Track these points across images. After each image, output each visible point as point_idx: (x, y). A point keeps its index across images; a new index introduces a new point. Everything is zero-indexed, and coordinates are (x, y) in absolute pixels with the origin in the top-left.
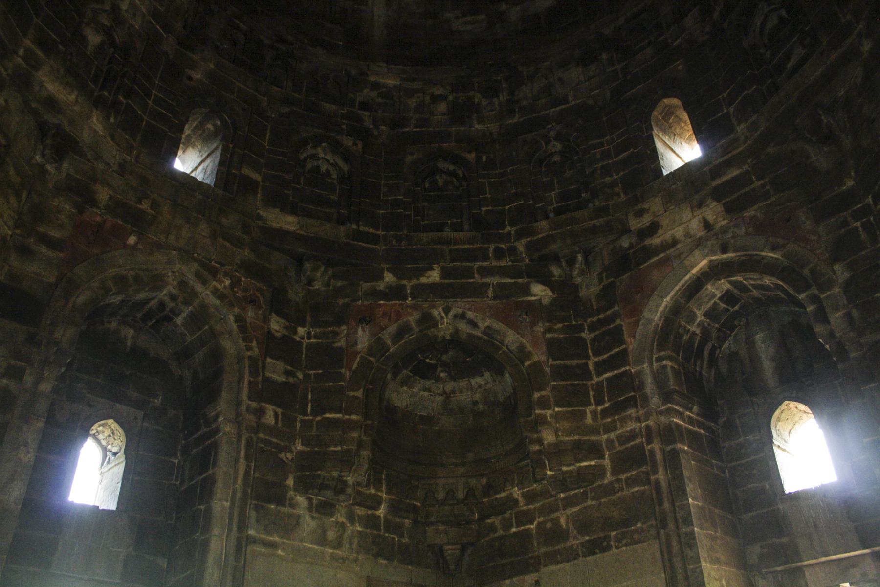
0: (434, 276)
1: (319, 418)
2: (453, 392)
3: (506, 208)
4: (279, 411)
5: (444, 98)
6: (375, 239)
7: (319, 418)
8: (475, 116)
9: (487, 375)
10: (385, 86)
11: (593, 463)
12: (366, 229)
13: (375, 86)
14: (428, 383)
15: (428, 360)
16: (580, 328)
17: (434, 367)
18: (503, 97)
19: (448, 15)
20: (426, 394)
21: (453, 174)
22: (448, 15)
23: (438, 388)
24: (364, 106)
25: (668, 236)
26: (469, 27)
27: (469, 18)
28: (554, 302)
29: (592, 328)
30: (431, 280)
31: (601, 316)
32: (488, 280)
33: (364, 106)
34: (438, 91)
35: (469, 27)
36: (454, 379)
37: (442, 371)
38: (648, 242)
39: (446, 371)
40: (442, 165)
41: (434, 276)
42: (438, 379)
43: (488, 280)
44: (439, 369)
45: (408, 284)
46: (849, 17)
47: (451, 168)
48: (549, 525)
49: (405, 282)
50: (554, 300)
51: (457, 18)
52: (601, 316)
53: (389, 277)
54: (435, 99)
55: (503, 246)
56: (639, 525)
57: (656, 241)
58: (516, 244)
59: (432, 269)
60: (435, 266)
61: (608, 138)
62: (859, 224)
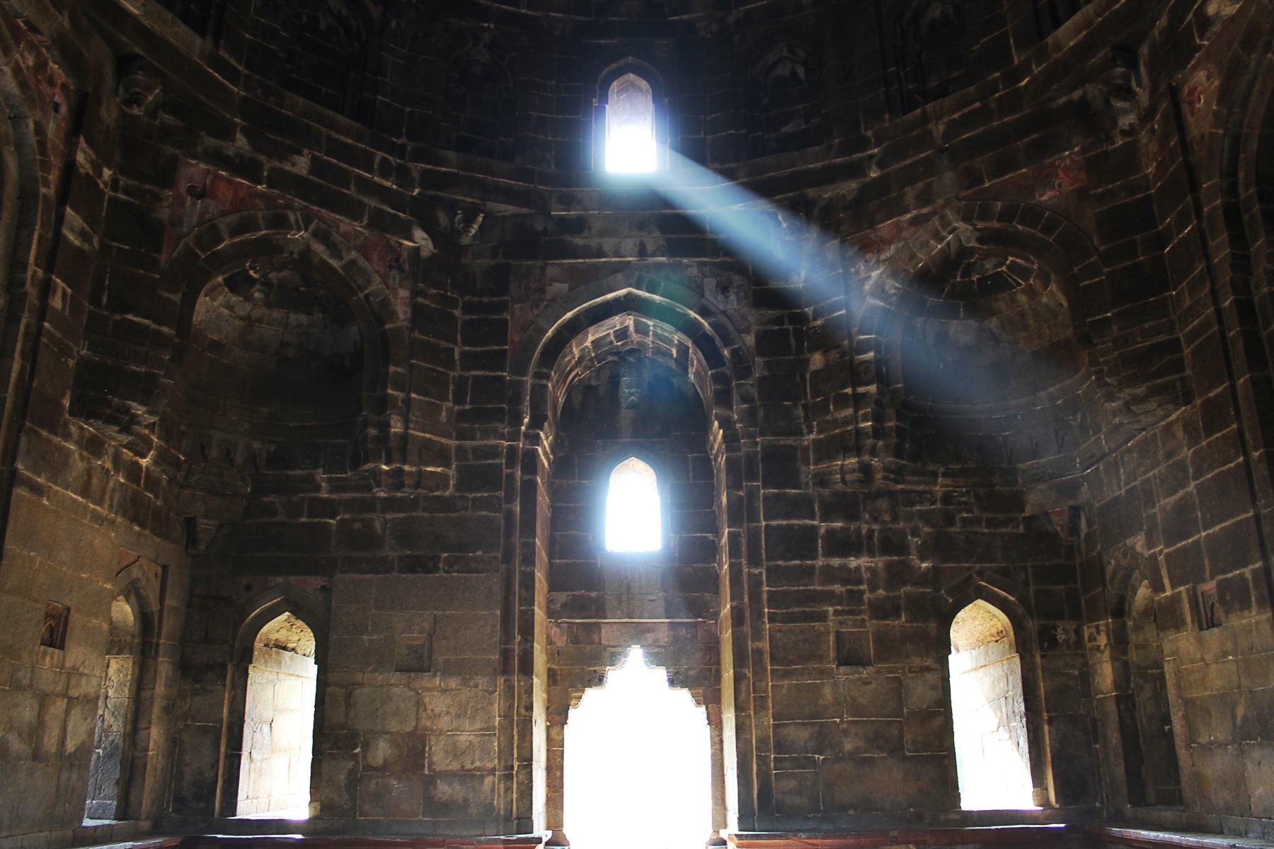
0: (301, 165)
1: (117, 317)
2: (260, 321)
3: (408, 109)
4: (69, 290)
6: (233, 75)
7: (117, 317)
9: (318, 316)
11: (439, 470)
12: (226, 56)
14: (234, 299)
15: (251, 272)
16: (453, 303)
17: (252, 281)
20: (226, 312)
23: (244, 308)
25: (594, 242)
28: (433, 258)
29: (468, 309)
30: (296, 170)
31: (485, 299)
32: (365, 200)
36: (268, 304)
37: (259, 290)
38: (567, 238)
39: (263, 292)
41: (301, 165)
42: (248, 298)
43: (365, 200)
44: (257, 286)
45: (268, 164)
46: (869, 133)
48: (357, 526)
49: (263, 158)
50: (434, 255)
52: (485, 299)
53: (241, 141)
55: (391, 158)
56: (479, 553)
57: (579, 241)
58: (410, 164)
59: (300, 154)
60: (306, 151)
61: (553, 83)
62: (791, 328)
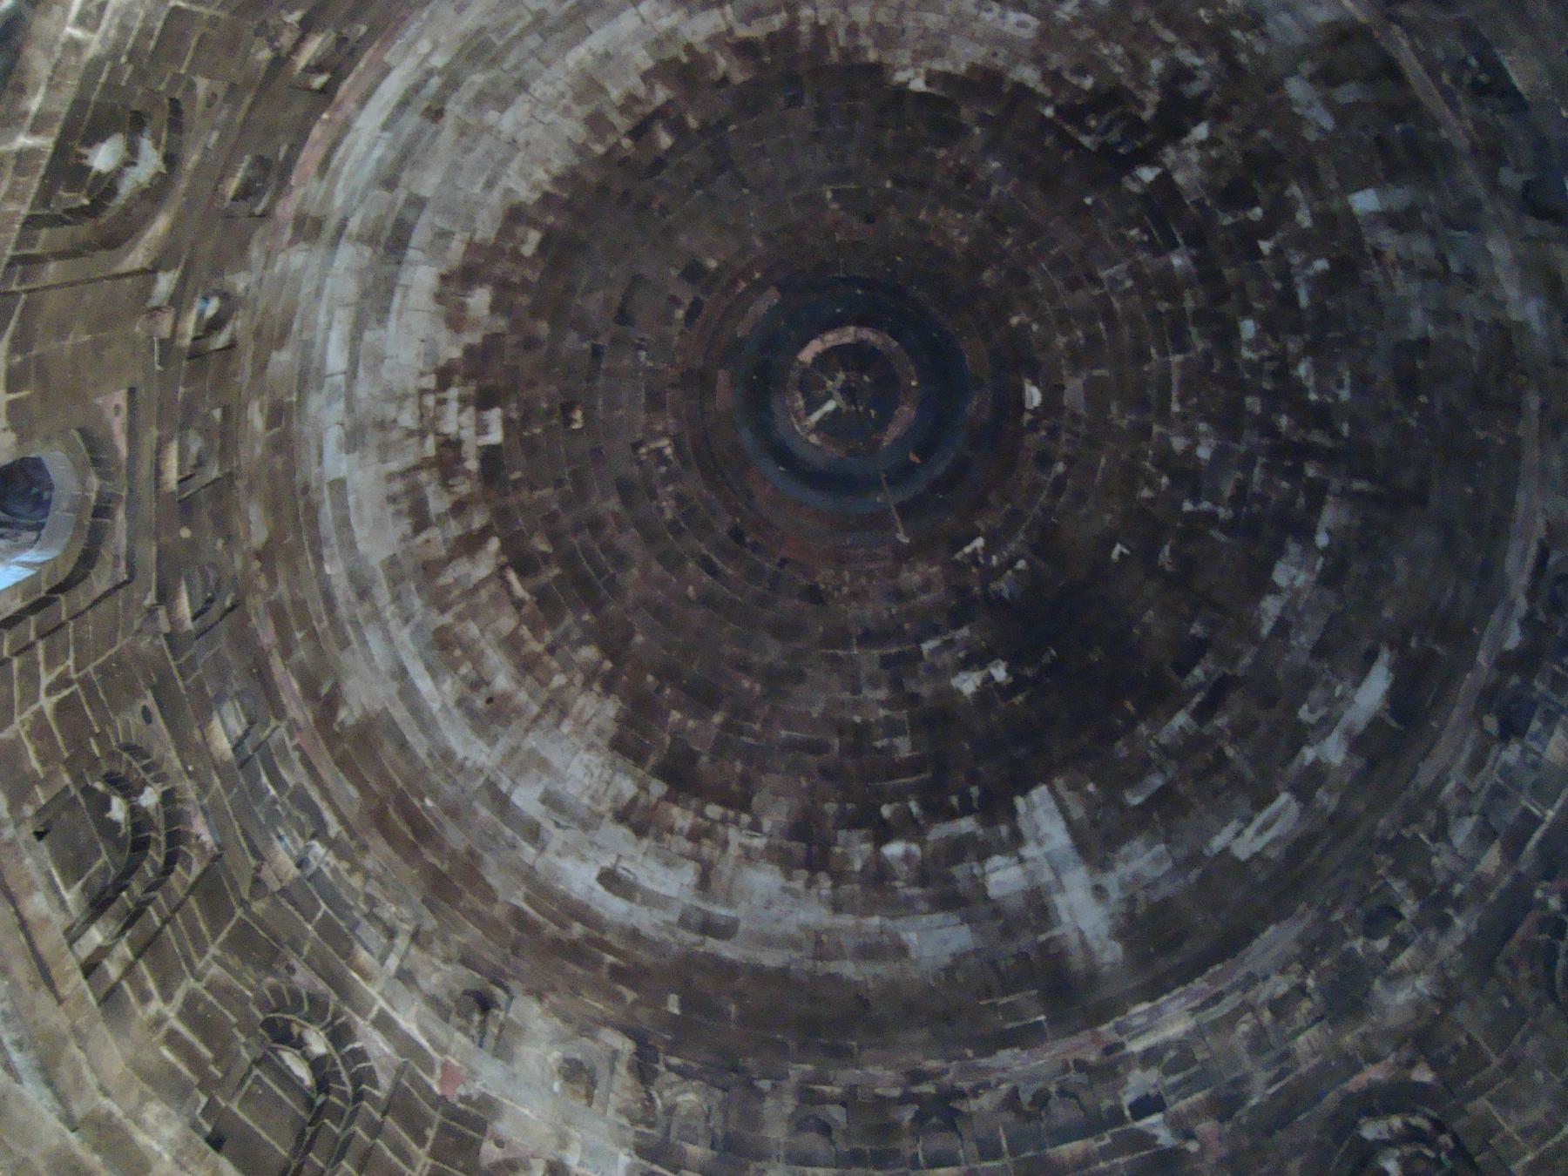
5: (1300, 991)
8: (1377, 984)
10: (1168, 1045)
13: (1150, 1057)
18: (1409, 907)
19: (1218, 842)
21: (1413, 1135)
22: (1218, 842)
24: (1145, 1106)
26: (1269, 835)
27: (1260, 819)
33: (1145, 1106)
34: (1280, 986)
35: (1269, 835)
40: (1371, 1131)
47: (1396, 1122)
51: (1239, 834)
54: (1280, 1007)
